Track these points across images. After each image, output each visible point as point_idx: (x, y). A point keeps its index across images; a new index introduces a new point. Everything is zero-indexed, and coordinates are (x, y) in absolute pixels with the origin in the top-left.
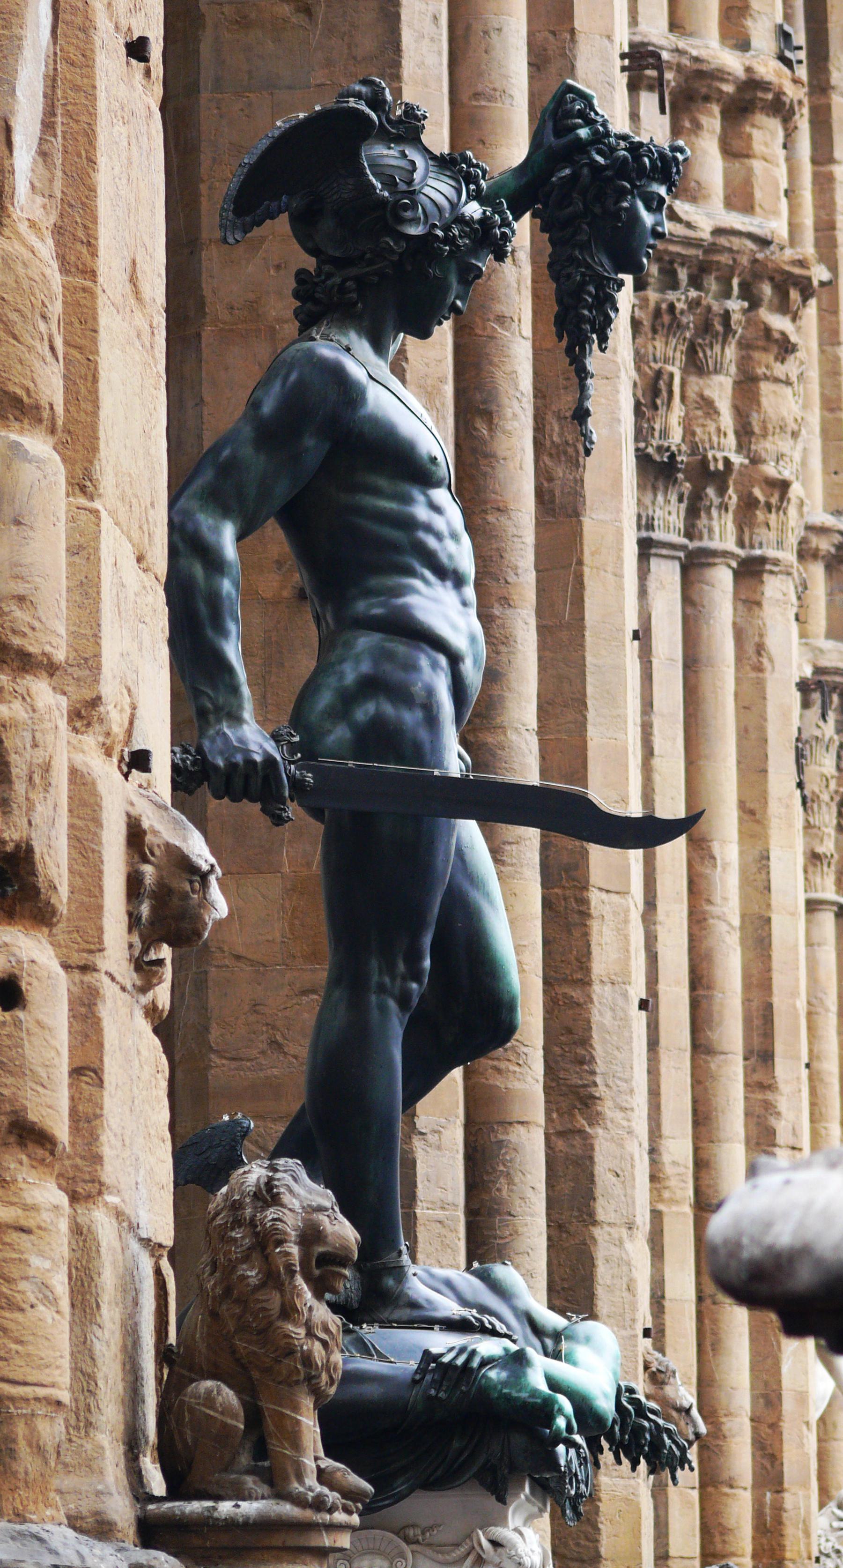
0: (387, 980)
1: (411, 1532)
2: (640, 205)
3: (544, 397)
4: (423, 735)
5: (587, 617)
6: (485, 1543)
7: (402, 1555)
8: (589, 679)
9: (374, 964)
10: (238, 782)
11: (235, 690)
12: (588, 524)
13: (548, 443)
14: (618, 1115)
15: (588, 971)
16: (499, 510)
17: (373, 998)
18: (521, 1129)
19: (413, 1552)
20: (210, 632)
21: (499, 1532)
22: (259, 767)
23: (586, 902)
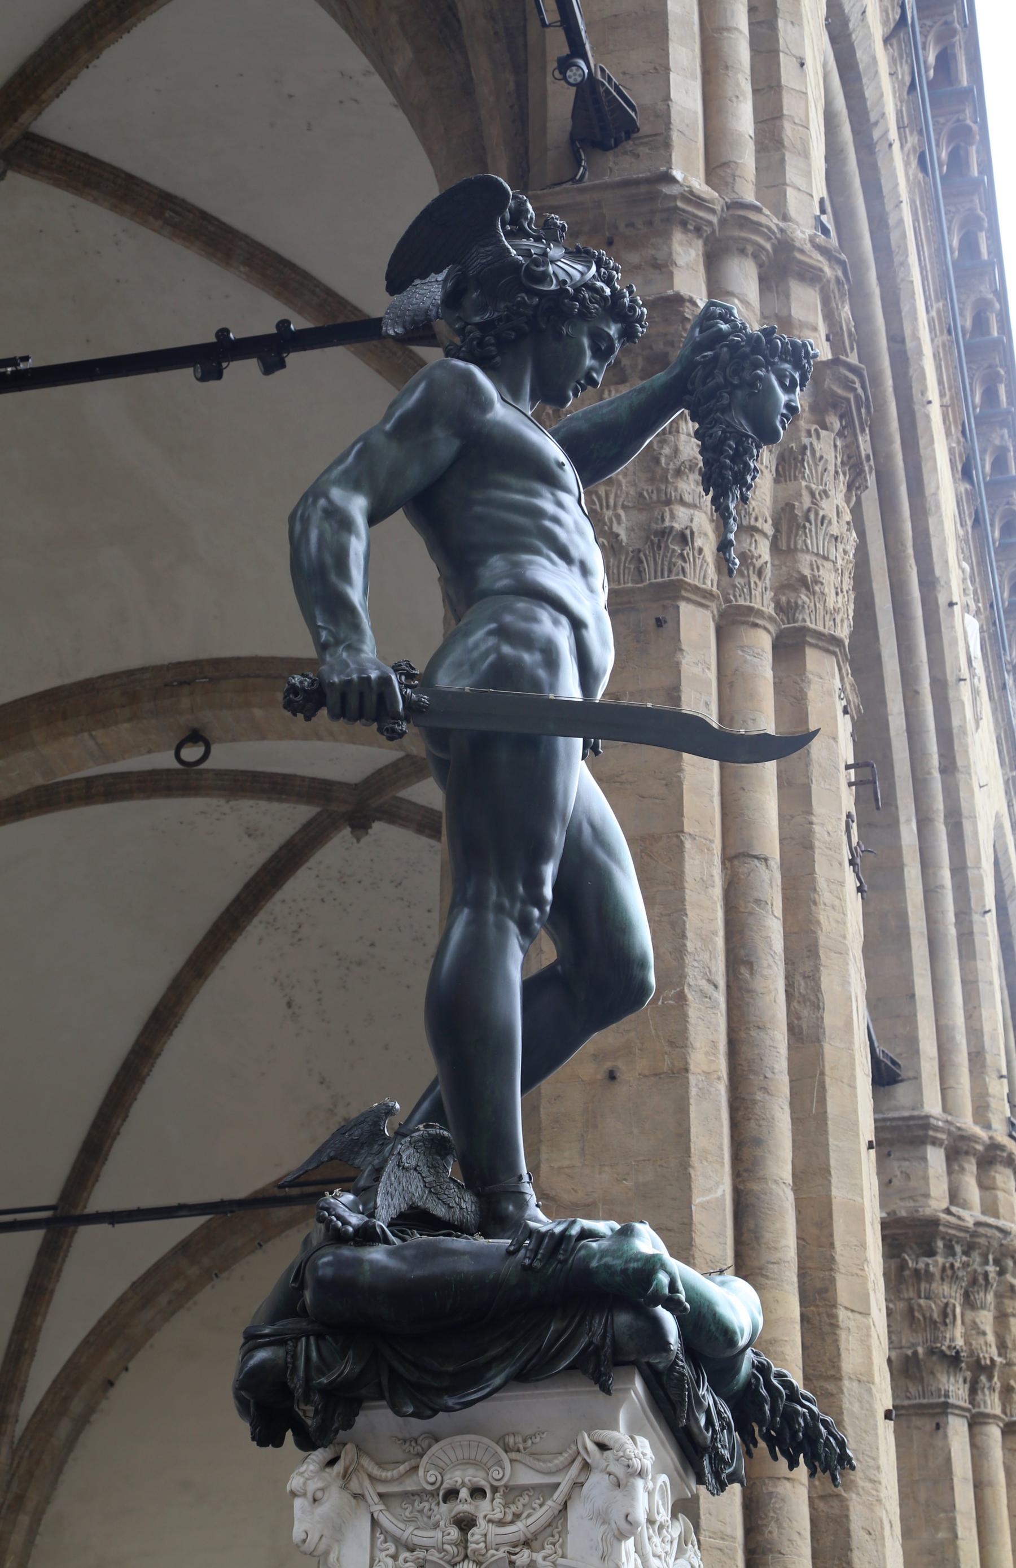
0: (507, 903)
1: (511, 1440)
2: (773, 378)
3: (793, 964)
4: (542, 673)
5: (829, 1110)
6: (590, 1445)
7: (499, 1463)
8: (832, 1154)
9: (493, 886)
10: (353, 701)
11: (356, 627)
12: (827, 1048)
13: (797, 994)
14: (868, 1485)
15: (839, 1369)
16: (759, 1027)
17: (491, 917)
18: (788, 1485)
19: (511, 1461)
20: (333, 578)
21: (606, 1435)
22: (373, 684)
23: (835, 1316)
